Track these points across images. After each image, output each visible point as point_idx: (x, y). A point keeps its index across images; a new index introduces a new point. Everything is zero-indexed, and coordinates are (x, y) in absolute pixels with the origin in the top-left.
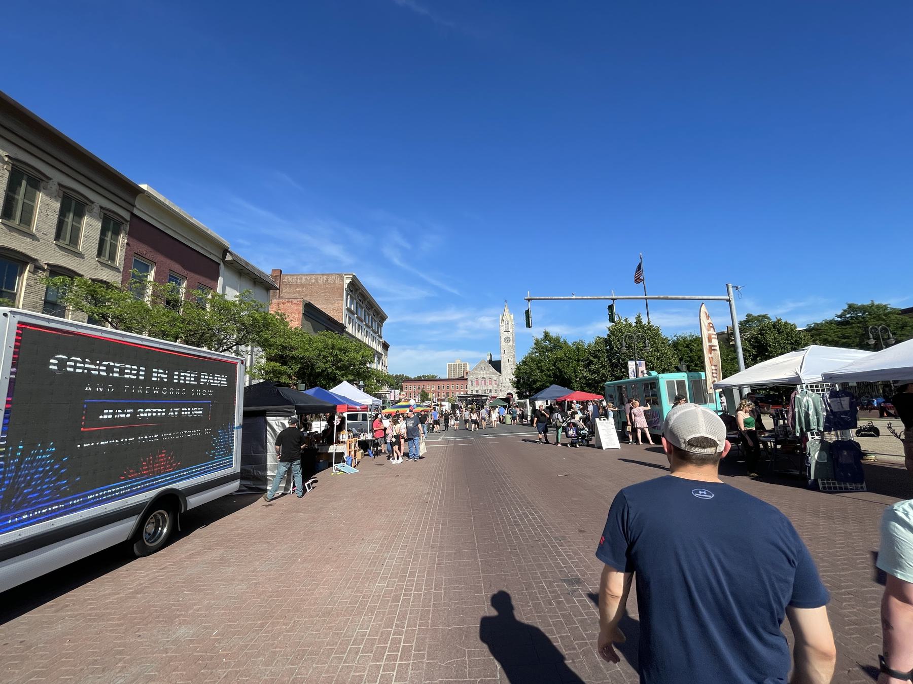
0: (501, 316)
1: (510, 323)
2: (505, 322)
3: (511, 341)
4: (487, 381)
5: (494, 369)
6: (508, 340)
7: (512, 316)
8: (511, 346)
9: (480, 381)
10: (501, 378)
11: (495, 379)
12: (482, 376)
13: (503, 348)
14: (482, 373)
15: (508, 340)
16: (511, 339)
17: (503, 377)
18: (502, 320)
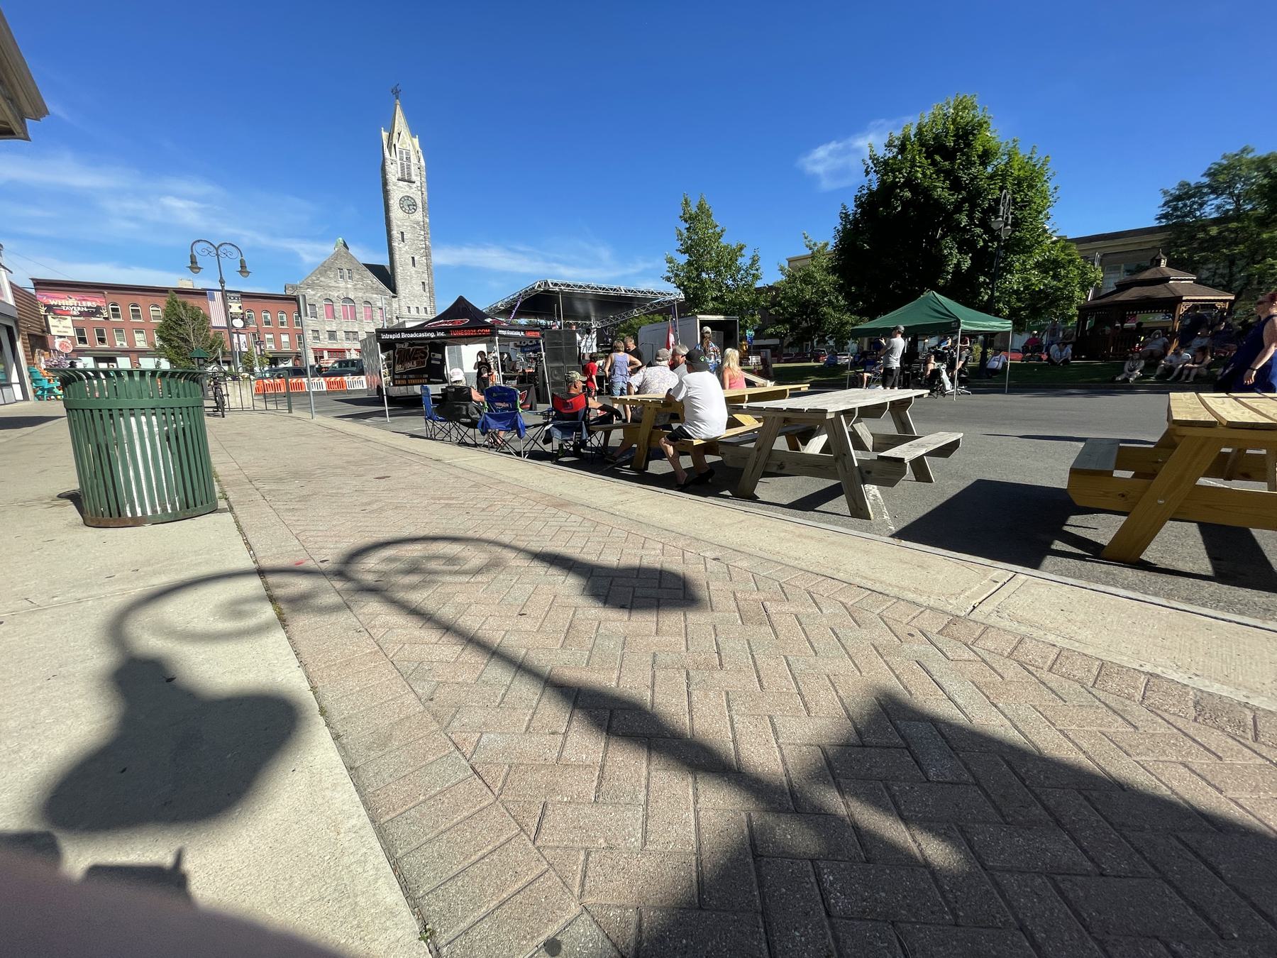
0: (385, 135)
1: (414, 160)
2: (401, 153)
3: (420, 209)
4: (360, 309)
5: (375, 280)
6: (409, 205)
7: (416, 141)
8: (418, 223)
9: (338, 306)
10: (395, 305)
11: (379, 304)
12: (342, 294)
13: (398, 226)
14: (343, 287)
15: (409, 205)
16: (420, 205)
17: (402, 303)
18: (391, 145)
